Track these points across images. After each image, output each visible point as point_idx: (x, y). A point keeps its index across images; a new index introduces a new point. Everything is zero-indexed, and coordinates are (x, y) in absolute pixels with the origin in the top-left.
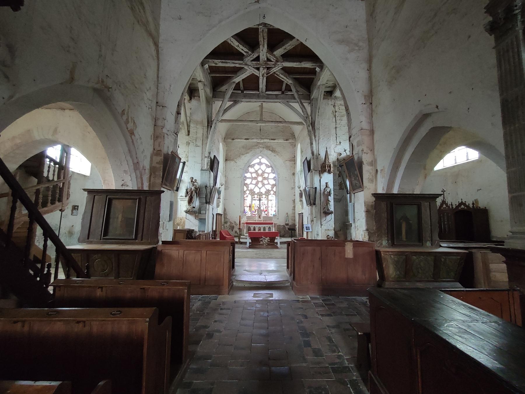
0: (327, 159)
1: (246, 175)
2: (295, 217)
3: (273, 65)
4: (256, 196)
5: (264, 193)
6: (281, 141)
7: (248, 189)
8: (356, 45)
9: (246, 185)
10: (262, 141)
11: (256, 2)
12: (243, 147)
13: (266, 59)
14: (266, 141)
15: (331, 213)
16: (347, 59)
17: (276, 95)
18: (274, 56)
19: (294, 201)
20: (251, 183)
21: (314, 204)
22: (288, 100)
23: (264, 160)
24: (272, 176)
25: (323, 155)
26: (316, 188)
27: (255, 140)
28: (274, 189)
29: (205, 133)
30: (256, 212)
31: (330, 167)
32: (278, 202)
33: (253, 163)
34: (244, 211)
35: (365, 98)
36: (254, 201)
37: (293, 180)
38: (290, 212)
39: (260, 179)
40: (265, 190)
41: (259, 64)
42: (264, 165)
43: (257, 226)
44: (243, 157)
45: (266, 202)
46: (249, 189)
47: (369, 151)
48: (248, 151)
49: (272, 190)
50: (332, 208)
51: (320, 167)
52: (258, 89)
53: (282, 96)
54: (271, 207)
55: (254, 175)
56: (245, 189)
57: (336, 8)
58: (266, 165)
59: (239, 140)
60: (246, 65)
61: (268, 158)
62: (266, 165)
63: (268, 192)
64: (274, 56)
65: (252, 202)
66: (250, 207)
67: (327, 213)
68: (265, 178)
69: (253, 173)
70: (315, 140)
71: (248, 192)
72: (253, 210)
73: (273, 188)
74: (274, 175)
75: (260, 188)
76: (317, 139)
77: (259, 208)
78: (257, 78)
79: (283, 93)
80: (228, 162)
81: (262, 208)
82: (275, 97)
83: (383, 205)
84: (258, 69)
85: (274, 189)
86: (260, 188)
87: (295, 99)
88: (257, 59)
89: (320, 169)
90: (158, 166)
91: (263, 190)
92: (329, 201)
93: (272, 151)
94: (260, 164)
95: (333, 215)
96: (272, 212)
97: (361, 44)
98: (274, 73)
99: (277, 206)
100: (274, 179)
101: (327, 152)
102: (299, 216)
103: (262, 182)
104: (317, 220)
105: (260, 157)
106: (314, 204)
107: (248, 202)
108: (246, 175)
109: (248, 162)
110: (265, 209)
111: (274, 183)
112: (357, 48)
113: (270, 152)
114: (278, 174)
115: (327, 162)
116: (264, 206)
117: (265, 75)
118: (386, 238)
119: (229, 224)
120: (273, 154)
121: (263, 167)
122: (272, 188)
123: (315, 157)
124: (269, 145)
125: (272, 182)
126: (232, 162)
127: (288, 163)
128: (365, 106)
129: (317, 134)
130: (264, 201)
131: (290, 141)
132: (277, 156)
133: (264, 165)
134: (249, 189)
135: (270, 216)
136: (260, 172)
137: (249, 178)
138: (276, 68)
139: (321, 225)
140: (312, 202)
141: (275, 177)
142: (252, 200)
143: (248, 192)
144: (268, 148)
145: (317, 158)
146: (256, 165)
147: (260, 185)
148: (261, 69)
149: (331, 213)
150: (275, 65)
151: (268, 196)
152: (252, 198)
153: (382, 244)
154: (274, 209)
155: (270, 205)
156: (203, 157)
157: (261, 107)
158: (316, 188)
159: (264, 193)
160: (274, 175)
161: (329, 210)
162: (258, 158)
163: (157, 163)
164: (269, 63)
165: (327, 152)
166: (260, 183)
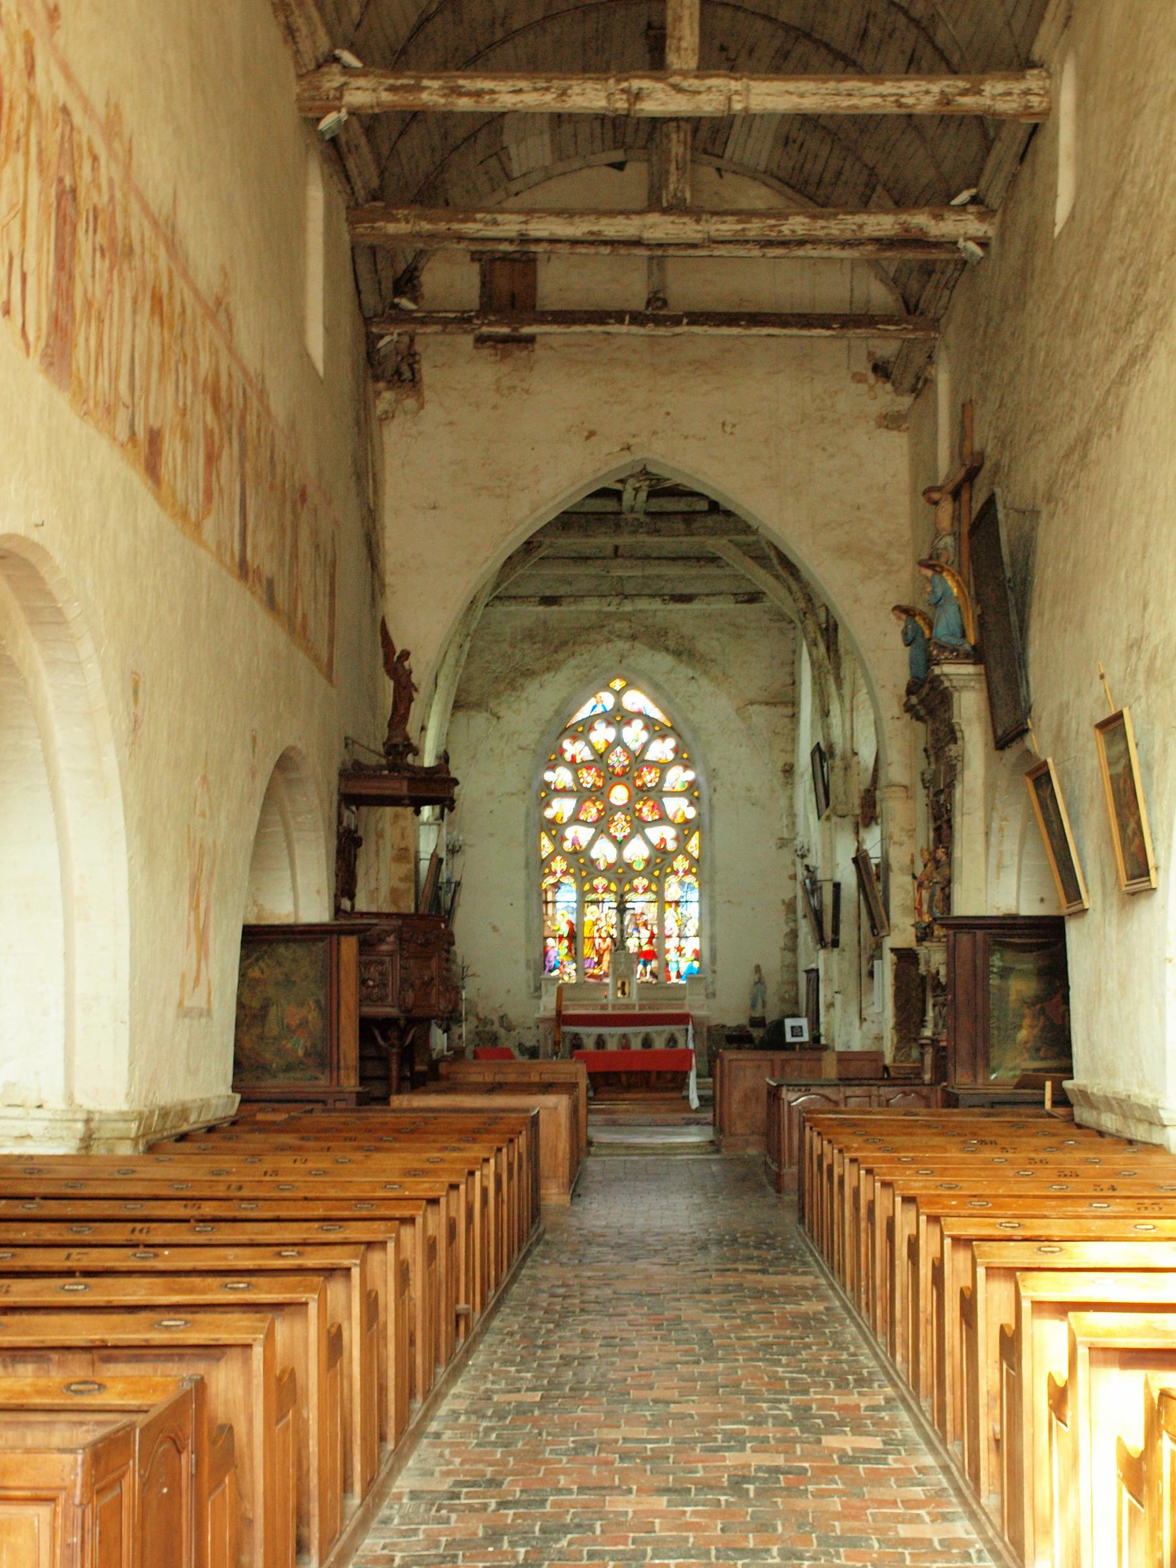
1: (549, 776)
2: (796, 983)
4: (600, 882)
5: (638, 866)
6: (723, 605)
7: (558, 851)
8: (882, 557)
9: (554, 827)
10: (628, 607)
12: (529, 635)
14: (643, 604)
20: (575, 819)
21: (835, 943)
23: (635, 700)
24: (678, 777)
27: (591, 605)
28: (693, 845)
30: (605, 965)
32: (712, 912)
33: (584, 713)
34: (542, 961)
36: (591, 912)
37: (783, 803)
39: (619, 795)
40: (645, 852)
42: (638, 724)
43: (613, 1034)
44: (532, 688)
45: (652, 912)
46: (567, 846)
47: (905, 839)
48: (561, 656)
49: (682, 850)
54: (680, 930)
55: (589, 778)
56: (547, 847)
57: (832, 456)
58: (650, 724)
59: (513, 608)
61: (657, 692)
62: (650, 724)
63: (660, 859)
65: (580, 912)
66: (572, 936)
68: (641, 792)
69: (587, 765)
70: (841, 697)
71: (559, 865)
72: (587, 951)
73: (687, 838)
74: (690, 775)
75: (620, 844)
76: (847, 689)
77: (619, 944)
81: (632, 944)
85: (693, 845)
86: (620, 844)
89: (858, 811)
90: (403, 886)
91: (637, 852)
93: (677, 654)
94: (619, 717)
96: (681, 960)
97: (893, 555)
99: (707, 932)
100: (691, 792)
102: (809, 981)
103: (627, 809)
104: (845, 1004)
105: (618, 684)
107: (561, 917)
108: (549, 776)
109: (558, 713)
111: (691, 813)
112: (883, 568)
113: (664, 661)
114: (712, 774)
116: (645, 934)
120: (684, 671)
121: (634, 734)
122: (682, 840)
125: (679, 808)
126: (480, 719)
127: (761, 716)
128: (897, 723)
129: (846, 671)
130: (639, 903)
132: (704, 682)
133: (638, 724)
134: (567, 846)
135: (674, 980)
136: (617, 759)
137: (564, 792)
139: (862, 1019)
141: (692, 785)
142: (583, 902)
143: (559, 865)
144: (656, 637)
146: (600, 726)
147: (620, 827)
151: (660, 881)
152: (582, 894)
153: (909, 1055)
154: (692, 944)
155: (671, 925)
159: (638, 866)
160: (690, 775)
162: (606, 687)
163: (401, 879)
166: (619, 816)
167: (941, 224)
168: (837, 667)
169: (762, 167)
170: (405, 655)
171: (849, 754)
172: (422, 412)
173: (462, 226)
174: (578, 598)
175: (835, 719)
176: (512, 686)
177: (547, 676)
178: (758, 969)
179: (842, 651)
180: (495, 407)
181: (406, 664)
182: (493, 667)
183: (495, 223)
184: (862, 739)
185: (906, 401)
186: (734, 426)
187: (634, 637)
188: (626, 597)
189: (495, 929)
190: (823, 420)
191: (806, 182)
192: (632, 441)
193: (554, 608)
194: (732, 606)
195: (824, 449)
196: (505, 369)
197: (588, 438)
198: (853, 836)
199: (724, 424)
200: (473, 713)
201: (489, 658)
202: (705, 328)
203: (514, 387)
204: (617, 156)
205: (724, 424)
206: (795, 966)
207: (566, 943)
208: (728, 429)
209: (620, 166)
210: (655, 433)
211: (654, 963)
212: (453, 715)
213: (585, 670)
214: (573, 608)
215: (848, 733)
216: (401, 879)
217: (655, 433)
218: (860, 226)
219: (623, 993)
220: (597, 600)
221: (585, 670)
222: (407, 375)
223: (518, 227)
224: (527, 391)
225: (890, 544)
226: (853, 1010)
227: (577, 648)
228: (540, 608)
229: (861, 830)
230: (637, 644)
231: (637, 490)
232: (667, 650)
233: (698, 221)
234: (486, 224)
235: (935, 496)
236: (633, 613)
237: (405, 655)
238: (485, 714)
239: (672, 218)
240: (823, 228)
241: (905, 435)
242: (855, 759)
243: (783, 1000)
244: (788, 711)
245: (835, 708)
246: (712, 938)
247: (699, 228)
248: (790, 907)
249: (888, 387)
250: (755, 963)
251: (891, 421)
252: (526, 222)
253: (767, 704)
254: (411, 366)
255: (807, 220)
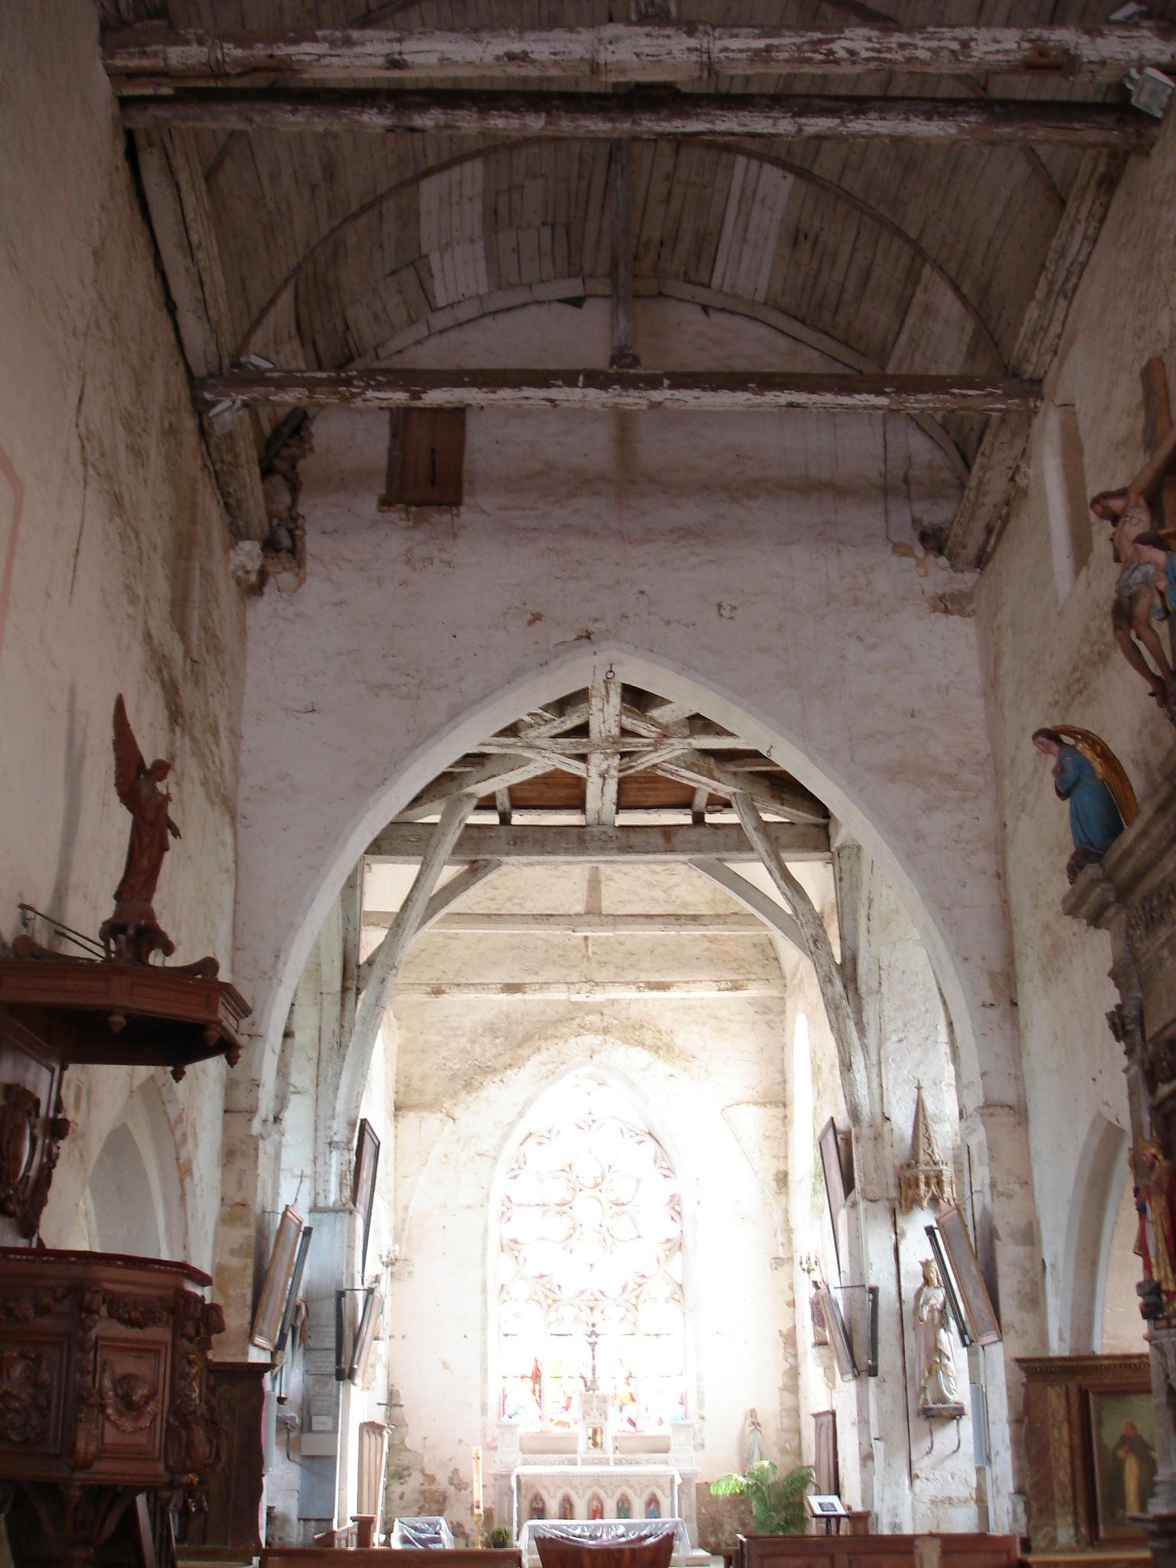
0: (922, 1141)
2: (798, 1431)
3: (649, 745)
8: (950, 779)
10: (599, 996)
11: (579, 638)
12: (492, 1030)
13: (616, 731)
15: (957, 1413)
16: (919, 837)
17: (668, 831)
18: (654, 723)
19: (790, 1339)
21: (873, 1371)
22: (725, 855)
25: (902, 1121)
26: (874, 1291)
27: (558, 994)
29: (331, 1026)
31: (939, 1183)
35: (993, 985)
38: (770, 1405)
41: (585, 745)
47: (1016, 1187)
48: (525, 1051)
50: (959, 1390)
51: (892, 1181)
52: (580, 805)
53: (694, 835)
55: (558, 1191)
59: (471, 996)
60: (530, 747)
64: (654, 723)
67: (938, 1414)
70: (865, 1048)
78: (579, 783)
79: (698, 819)
80: (411, 1118)
81: (604, 1387)
82: (658, 840)
83: (1054, 1397)
84: (583, 758)
87: (752, 849)
88: (582, 730)
89: (893, 1193)
90: (236, 1262)
92: (940, 1353)
93: (655, 1049)
95: (967, 1425)
97: (967, 776)
98: (654, 766)
101: (920, 1105)
102: (819, 1428)
104: (888, 1455)
106: (873, 1371)
110: (623, 1393)
115: (923, 1157)
117: (614, 773)
118: (1070, 1519)
119: (415, 1482)
120: (661, 1067)
123: (865, 1130)
124: (635, 1012)
126: (433, 1121)
128: (991, 1012)
131: (754, 991)
138: (661, 752)
139: (912, 1477)
140: (862, 1363)
145: (877, 1137)
148: (596, 759)
149: (957, 1413)
150: (656, 746)
153: (1053, 1540)
156: (322, 1146)
157: (594, 884)
158: (874, 1291)
161: (943, 1400)
163: (233, 1252)
164: (630, 740)
165: (920, 1105)
167: (1100, 41)
168: (859, 1011)
169: (760, 297)
170: (161, 769)
171: (879, 1119)
172: (304, 588)
173: (292, 50)
174: (545, 985)
175: (860, 1075)
176: (469, 1086)
177: (509, 1072)
178: (753, 1413)
179: (863, 989)
180: (403, 583)
181: (160, 786)
182: (450, 1064)
183: (349, 42)
184: (894, 1101)
185: (969, 578)
186: (734, 608)
187: (606, 1031)
188: (597, 984)
189: (445, 1365)
190: (856, 602)
191: (820, 307)
192: (592, 627)
193: (518, 996)
194: (715, 994)
195: (860, 639)
196: (419, 536)
197: (530, 623)
198: (890, 1227)
199: (720, 606)
200: (425, 1114)
201: (445, 1054)
202: (697, 393)
203: (431, 559)
204: (573, 287)
205: (720, 606)
206: (795, 1412)
207: (529, 1383)
208: (726, 613)
209: (577, 302)
210: (624, 616)
211: (631, 1410)
212: (396, 1116)
213: (551, 1067)
214: (538, 996)
215: (876, 1093)
216: (233, 1252)
217: (624, 616)
218: (965, 44)
219: (595, 1444)
220: (564, 987)
221: (551, 1067)
222: (286, 542)
223: (386, 48)
224: (449, 564)
225: (961, 762)
226: (901, 1463)
227: (543, 1043)
228: (503, 996)
229: (899, 1219)
230: (609, 1038)
231: (603, 776)
232: (641, 1043)
233: (690, 34)
234: (332, 44)
235: (1116, 505)
236: (602, 1004)
237: (161, 769)
238: (439, 1115)
239: (649, 29)
240: (902, 46)
241: (970, 620)
242: (887, 1125)
243: (783, 1451)
244: (778, 1111)
245: (858, 1061)
246: (699, 1378)
247: (693, 43)
248: (790, 1339)
249: (943, 561)
250: (748, 1407)
251: (947, 604)
252: (400, 41)
253: (756, 1103)
254: (291, 532)
255: (874, 33)
